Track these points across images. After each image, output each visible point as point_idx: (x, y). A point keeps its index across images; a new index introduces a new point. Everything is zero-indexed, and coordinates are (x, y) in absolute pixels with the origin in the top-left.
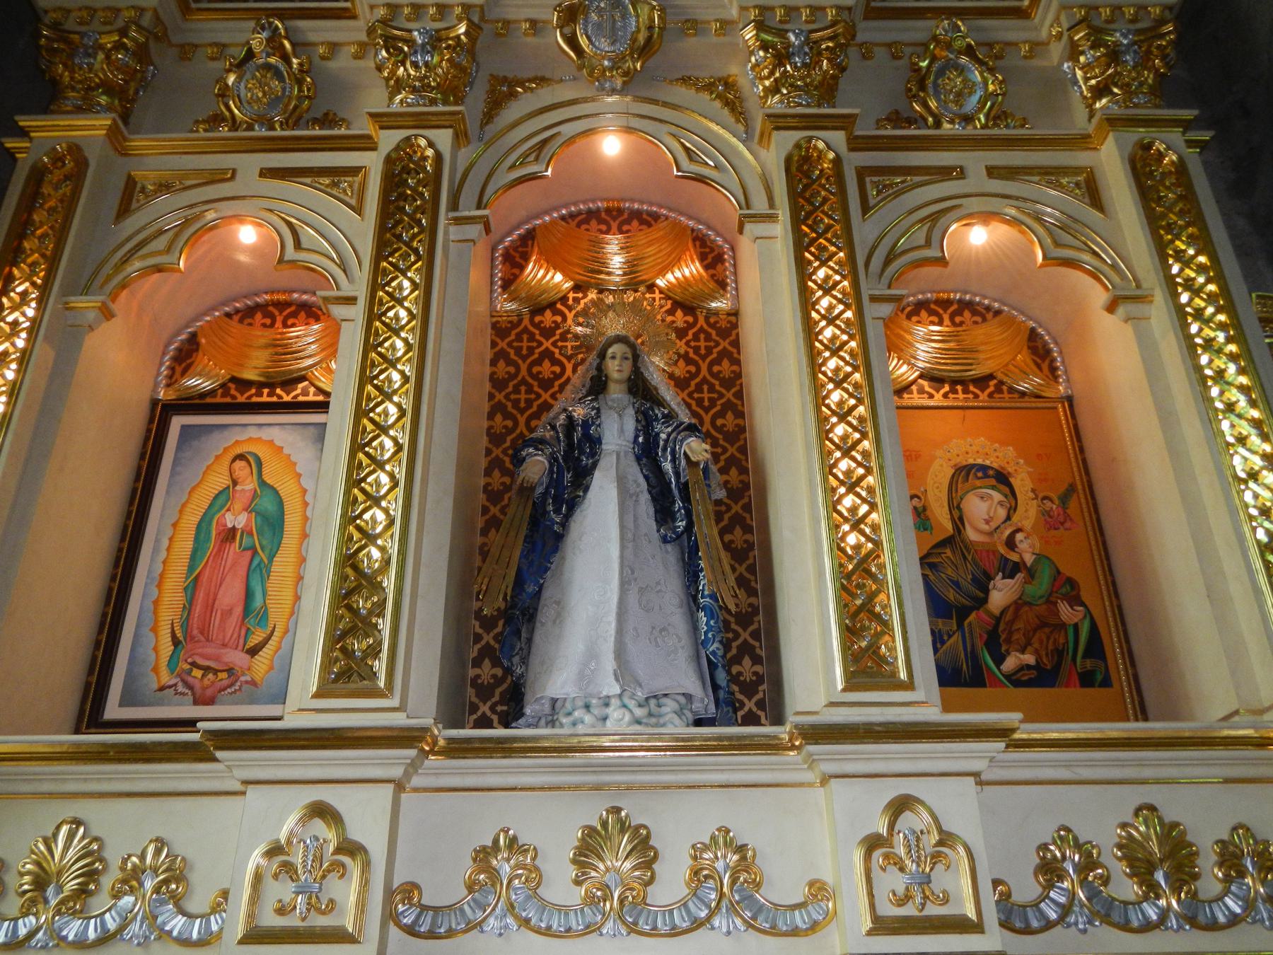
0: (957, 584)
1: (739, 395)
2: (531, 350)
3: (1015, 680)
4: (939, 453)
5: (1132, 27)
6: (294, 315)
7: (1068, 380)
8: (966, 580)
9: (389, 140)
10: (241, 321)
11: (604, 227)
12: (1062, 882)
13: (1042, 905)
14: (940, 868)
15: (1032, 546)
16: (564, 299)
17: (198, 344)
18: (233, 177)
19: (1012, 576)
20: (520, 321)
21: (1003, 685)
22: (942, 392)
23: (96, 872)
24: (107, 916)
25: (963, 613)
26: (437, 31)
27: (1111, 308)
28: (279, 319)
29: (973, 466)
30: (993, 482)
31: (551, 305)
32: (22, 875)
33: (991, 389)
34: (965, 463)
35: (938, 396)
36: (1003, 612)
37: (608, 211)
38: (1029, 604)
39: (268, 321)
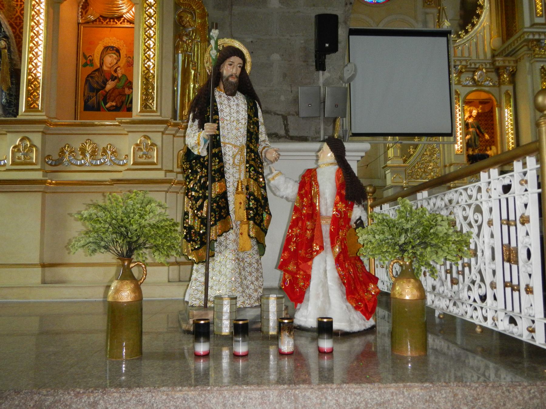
0: (97, 82)
3: (109, 110)
4: (100, 42)
8: (100, 81)
15: (122, 72)
19: (114, 81)
21: (105, 111)
22: (106, 21)
25: (98, 91)
29: (110, 46)
30: (115, 52)
33: (122, 21)
34: (107, 45)
35: (105, 23)
36: (109, 91)
38: (117, 89)
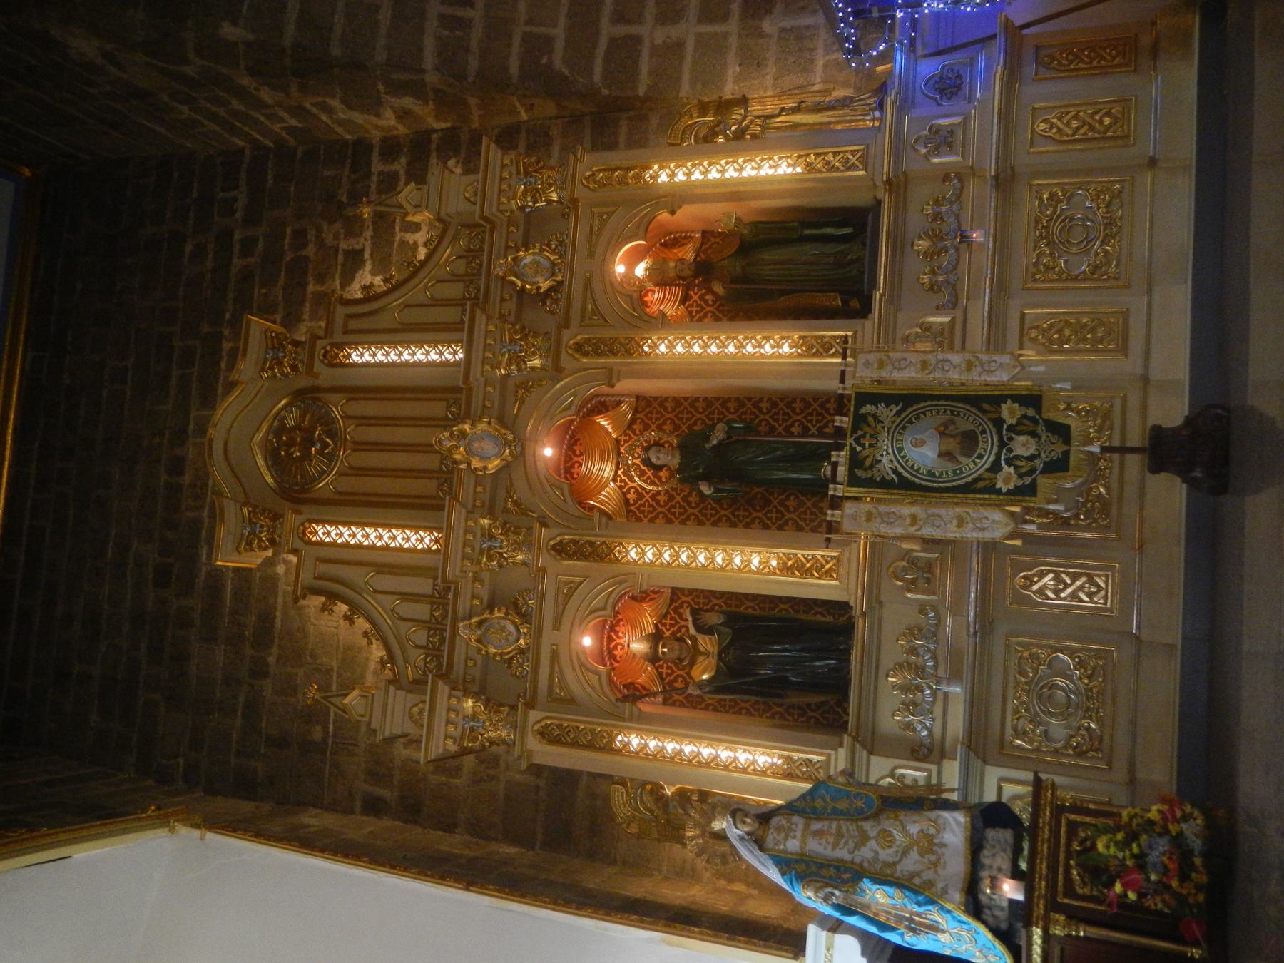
1: (686, 399)
2: (650, 506)
5: (514, 176)
6: (617, 633)
7: (692, 231)
9: (547, 560)
10: (618, 662)
11: (577, 465)
16: (621, 488)
17: (630, 683)
18: (556, 645)
20: (631, 511)
26: (483, 535)
27: (673, 213)
28: (618, 641)
31: (624, 494)
37: (566, 462)
39: (619, 647)
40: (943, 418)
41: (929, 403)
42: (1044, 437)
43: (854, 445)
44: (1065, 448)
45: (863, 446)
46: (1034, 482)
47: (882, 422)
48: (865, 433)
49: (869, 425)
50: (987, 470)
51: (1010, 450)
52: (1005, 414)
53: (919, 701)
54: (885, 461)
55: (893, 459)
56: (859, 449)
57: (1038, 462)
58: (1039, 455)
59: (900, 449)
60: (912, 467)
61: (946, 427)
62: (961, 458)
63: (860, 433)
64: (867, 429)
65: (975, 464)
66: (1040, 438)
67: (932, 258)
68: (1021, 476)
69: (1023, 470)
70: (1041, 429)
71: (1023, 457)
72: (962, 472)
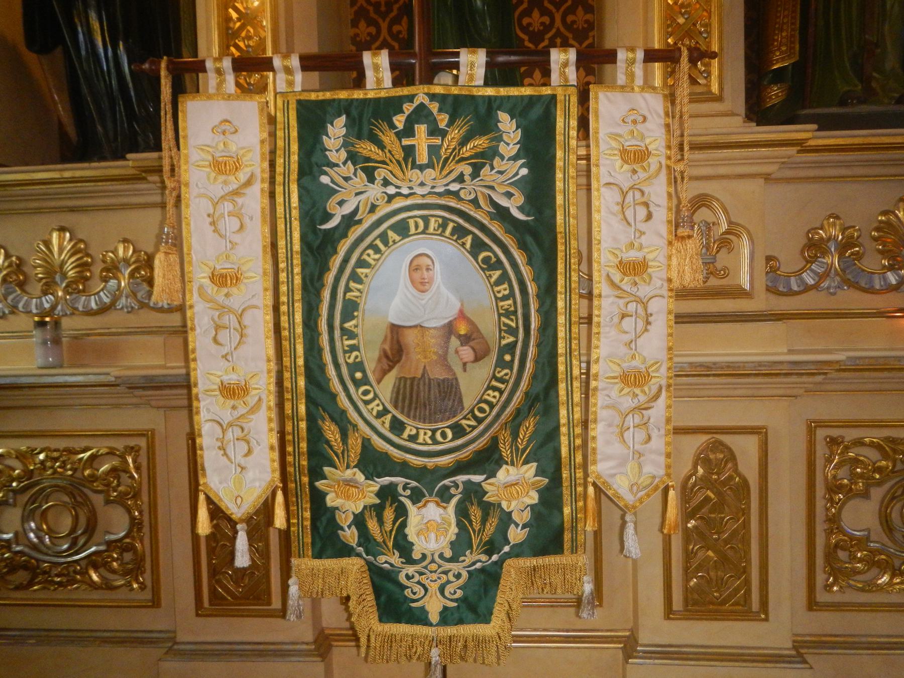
12: (824, 258)
13: (804, 275)
14: (724, 251)
23: (86, 264)
24: (102, 294)
32: (35, 267)
40: (488, 325)
41: (532, 288)
42: (455, 567)
43: (408, 108)
44: (434, 618)
45: (408, 131)
46: (345, 551)
47: (475, 174)
48: (443, 134)
49: (463, 142)
50: (367, 442)
51: (417, 497)
52: (505, 474)
53: (28, 288)
54: (375, 192)
55: (379, 213)
56: (399, 121)
57: (395, 559)
58: (410, 561)
59: (402, 229)
60: (361, 263)
61: (466, 340)
62: (390, 380)
63: (443, 120)
64: (455, 134)
65: (380, 415)
66: (453, 559)
67: (875, 239)
68: (359, 521)
69: (372, 525)
70: (475, 558)
71: (404, 525)
72: (357, 384)
